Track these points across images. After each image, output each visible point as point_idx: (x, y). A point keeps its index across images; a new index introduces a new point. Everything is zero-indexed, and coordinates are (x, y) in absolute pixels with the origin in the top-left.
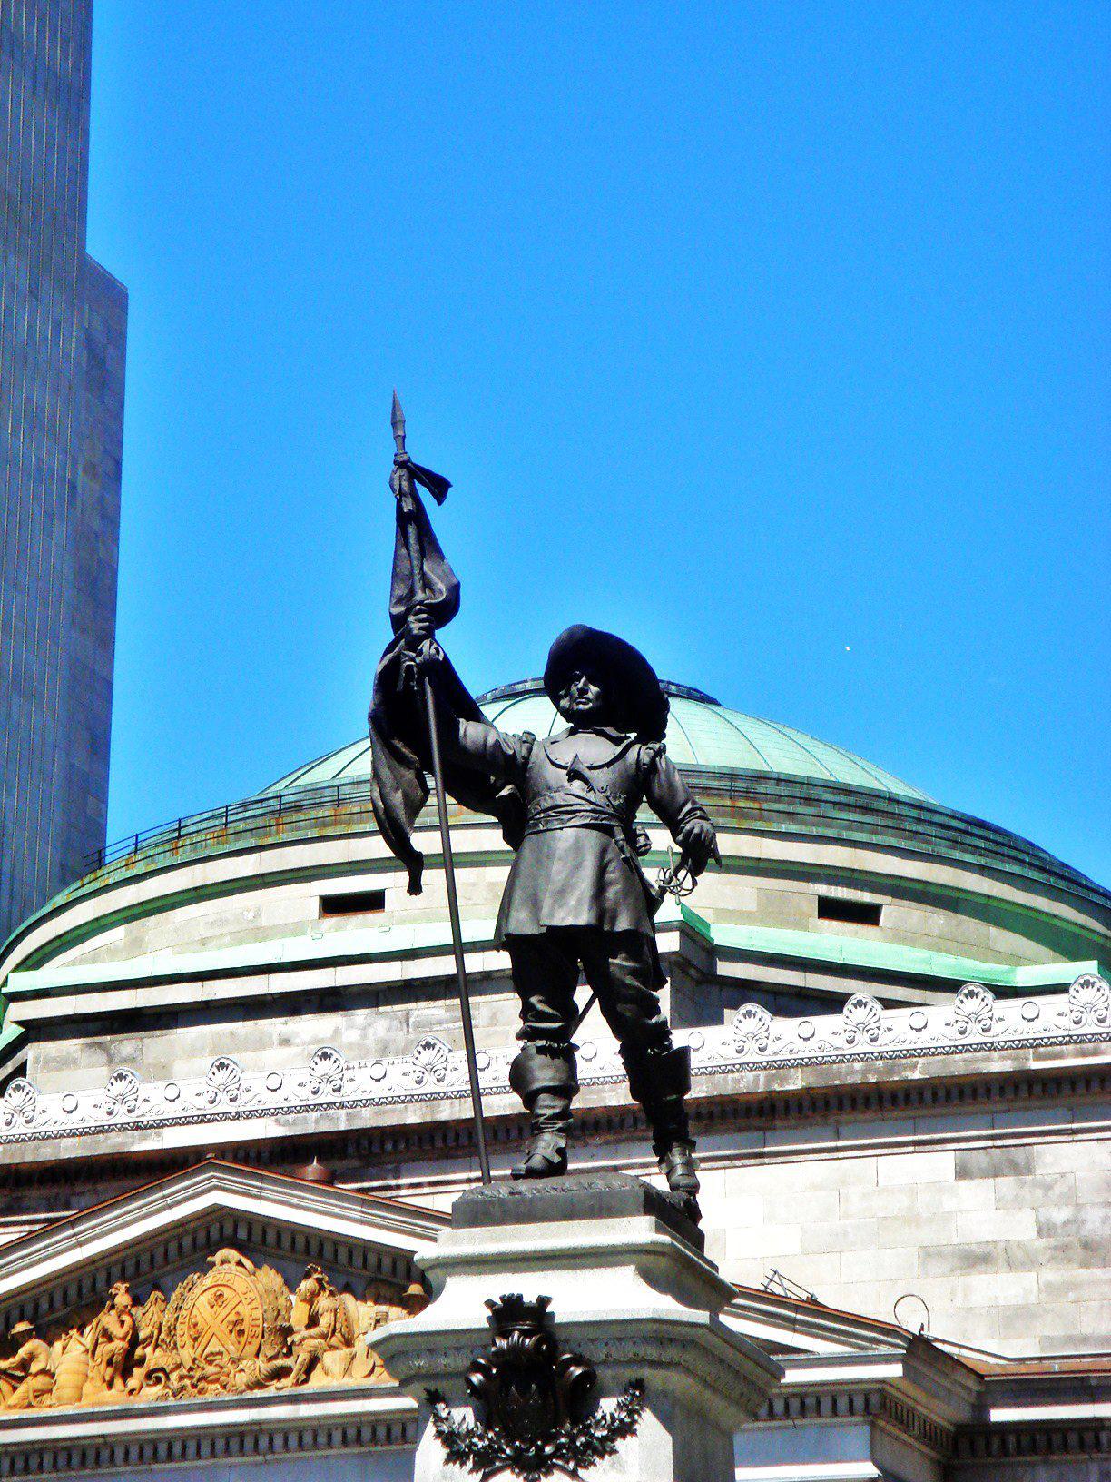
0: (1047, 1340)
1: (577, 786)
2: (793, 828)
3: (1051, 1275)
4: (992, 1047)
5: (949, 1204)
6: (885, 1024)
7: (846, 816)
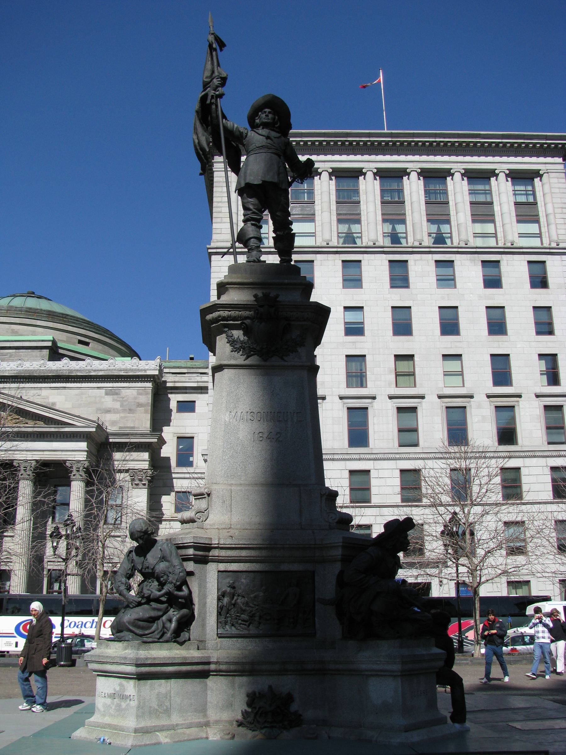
0: (120, 428)
1: (269, 141)
2: (75, 325)
3: (122, 415)
4: (115, 370)
5: (103, 400)
6: (94, 363)
7: (85, 324)
